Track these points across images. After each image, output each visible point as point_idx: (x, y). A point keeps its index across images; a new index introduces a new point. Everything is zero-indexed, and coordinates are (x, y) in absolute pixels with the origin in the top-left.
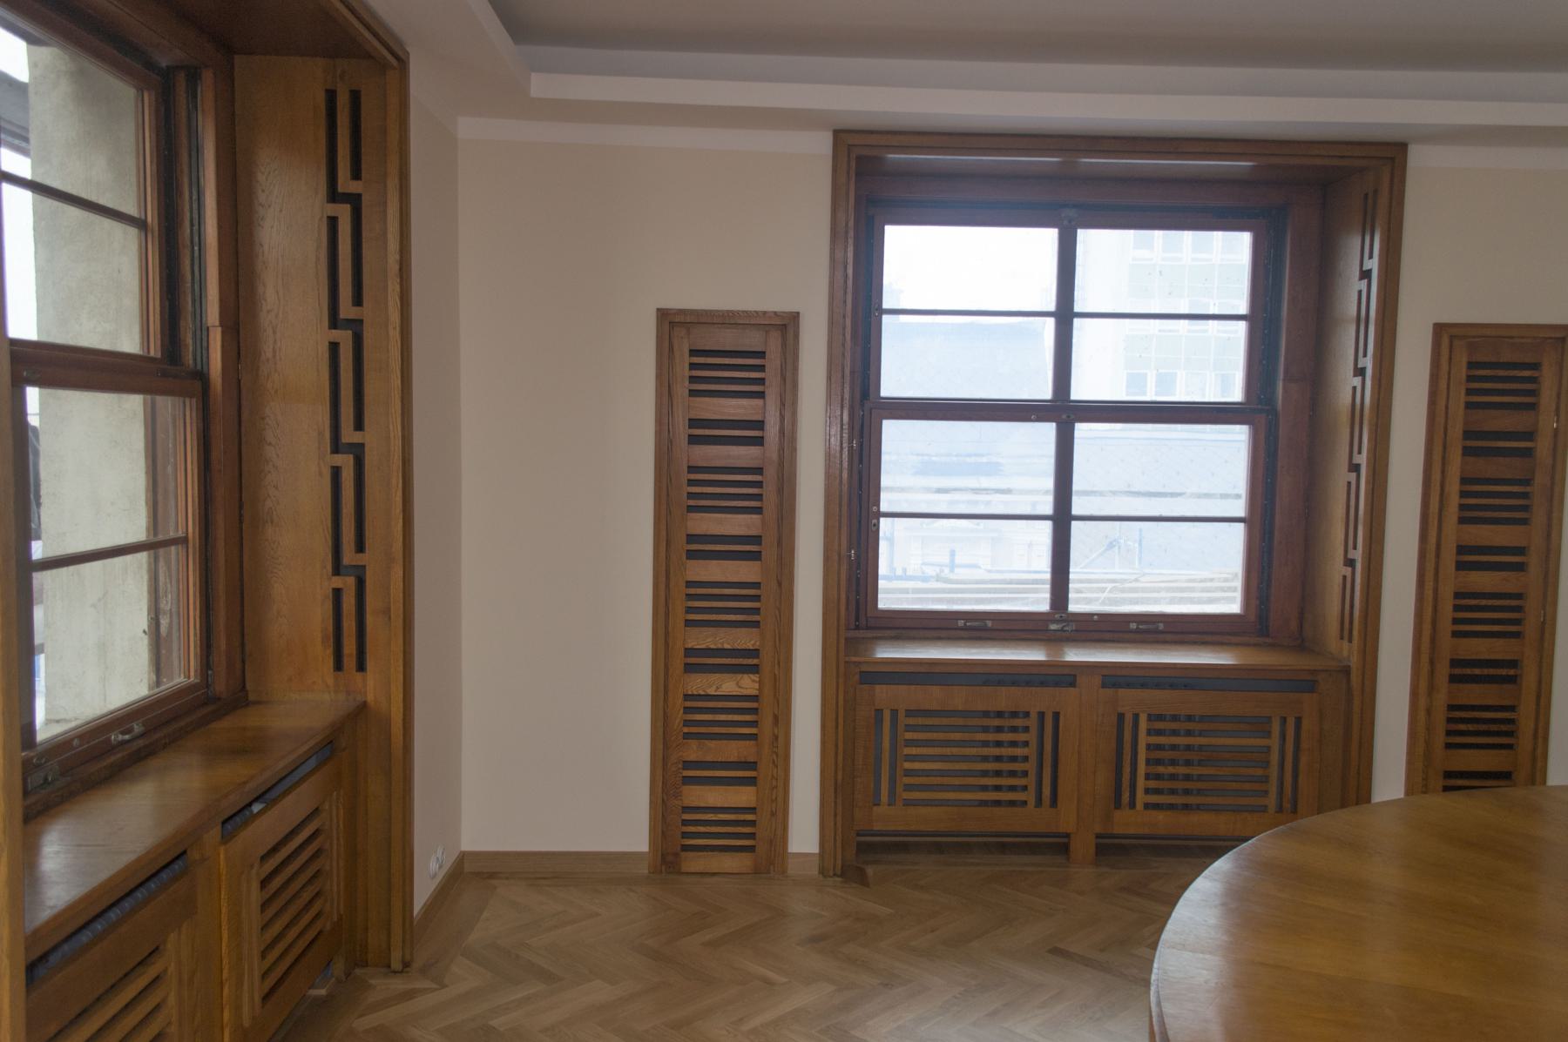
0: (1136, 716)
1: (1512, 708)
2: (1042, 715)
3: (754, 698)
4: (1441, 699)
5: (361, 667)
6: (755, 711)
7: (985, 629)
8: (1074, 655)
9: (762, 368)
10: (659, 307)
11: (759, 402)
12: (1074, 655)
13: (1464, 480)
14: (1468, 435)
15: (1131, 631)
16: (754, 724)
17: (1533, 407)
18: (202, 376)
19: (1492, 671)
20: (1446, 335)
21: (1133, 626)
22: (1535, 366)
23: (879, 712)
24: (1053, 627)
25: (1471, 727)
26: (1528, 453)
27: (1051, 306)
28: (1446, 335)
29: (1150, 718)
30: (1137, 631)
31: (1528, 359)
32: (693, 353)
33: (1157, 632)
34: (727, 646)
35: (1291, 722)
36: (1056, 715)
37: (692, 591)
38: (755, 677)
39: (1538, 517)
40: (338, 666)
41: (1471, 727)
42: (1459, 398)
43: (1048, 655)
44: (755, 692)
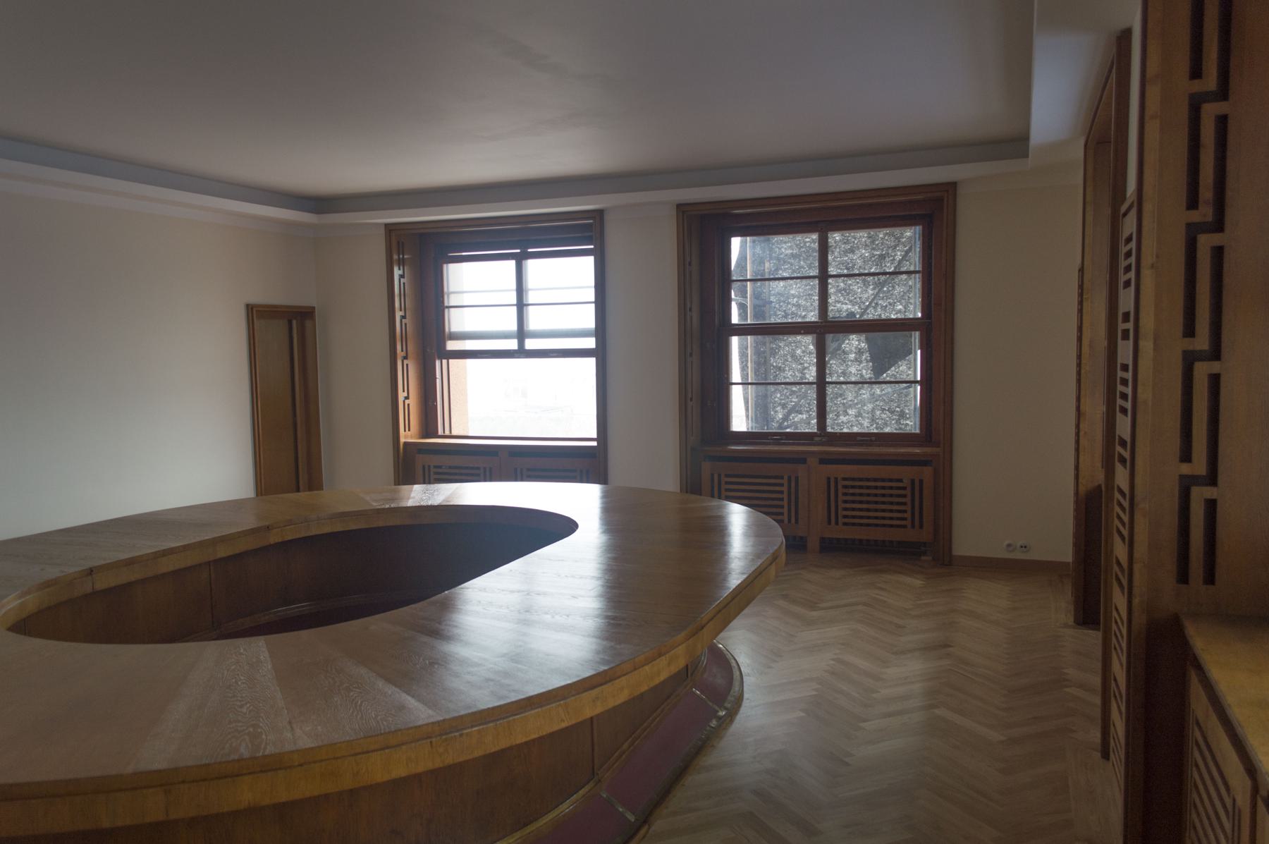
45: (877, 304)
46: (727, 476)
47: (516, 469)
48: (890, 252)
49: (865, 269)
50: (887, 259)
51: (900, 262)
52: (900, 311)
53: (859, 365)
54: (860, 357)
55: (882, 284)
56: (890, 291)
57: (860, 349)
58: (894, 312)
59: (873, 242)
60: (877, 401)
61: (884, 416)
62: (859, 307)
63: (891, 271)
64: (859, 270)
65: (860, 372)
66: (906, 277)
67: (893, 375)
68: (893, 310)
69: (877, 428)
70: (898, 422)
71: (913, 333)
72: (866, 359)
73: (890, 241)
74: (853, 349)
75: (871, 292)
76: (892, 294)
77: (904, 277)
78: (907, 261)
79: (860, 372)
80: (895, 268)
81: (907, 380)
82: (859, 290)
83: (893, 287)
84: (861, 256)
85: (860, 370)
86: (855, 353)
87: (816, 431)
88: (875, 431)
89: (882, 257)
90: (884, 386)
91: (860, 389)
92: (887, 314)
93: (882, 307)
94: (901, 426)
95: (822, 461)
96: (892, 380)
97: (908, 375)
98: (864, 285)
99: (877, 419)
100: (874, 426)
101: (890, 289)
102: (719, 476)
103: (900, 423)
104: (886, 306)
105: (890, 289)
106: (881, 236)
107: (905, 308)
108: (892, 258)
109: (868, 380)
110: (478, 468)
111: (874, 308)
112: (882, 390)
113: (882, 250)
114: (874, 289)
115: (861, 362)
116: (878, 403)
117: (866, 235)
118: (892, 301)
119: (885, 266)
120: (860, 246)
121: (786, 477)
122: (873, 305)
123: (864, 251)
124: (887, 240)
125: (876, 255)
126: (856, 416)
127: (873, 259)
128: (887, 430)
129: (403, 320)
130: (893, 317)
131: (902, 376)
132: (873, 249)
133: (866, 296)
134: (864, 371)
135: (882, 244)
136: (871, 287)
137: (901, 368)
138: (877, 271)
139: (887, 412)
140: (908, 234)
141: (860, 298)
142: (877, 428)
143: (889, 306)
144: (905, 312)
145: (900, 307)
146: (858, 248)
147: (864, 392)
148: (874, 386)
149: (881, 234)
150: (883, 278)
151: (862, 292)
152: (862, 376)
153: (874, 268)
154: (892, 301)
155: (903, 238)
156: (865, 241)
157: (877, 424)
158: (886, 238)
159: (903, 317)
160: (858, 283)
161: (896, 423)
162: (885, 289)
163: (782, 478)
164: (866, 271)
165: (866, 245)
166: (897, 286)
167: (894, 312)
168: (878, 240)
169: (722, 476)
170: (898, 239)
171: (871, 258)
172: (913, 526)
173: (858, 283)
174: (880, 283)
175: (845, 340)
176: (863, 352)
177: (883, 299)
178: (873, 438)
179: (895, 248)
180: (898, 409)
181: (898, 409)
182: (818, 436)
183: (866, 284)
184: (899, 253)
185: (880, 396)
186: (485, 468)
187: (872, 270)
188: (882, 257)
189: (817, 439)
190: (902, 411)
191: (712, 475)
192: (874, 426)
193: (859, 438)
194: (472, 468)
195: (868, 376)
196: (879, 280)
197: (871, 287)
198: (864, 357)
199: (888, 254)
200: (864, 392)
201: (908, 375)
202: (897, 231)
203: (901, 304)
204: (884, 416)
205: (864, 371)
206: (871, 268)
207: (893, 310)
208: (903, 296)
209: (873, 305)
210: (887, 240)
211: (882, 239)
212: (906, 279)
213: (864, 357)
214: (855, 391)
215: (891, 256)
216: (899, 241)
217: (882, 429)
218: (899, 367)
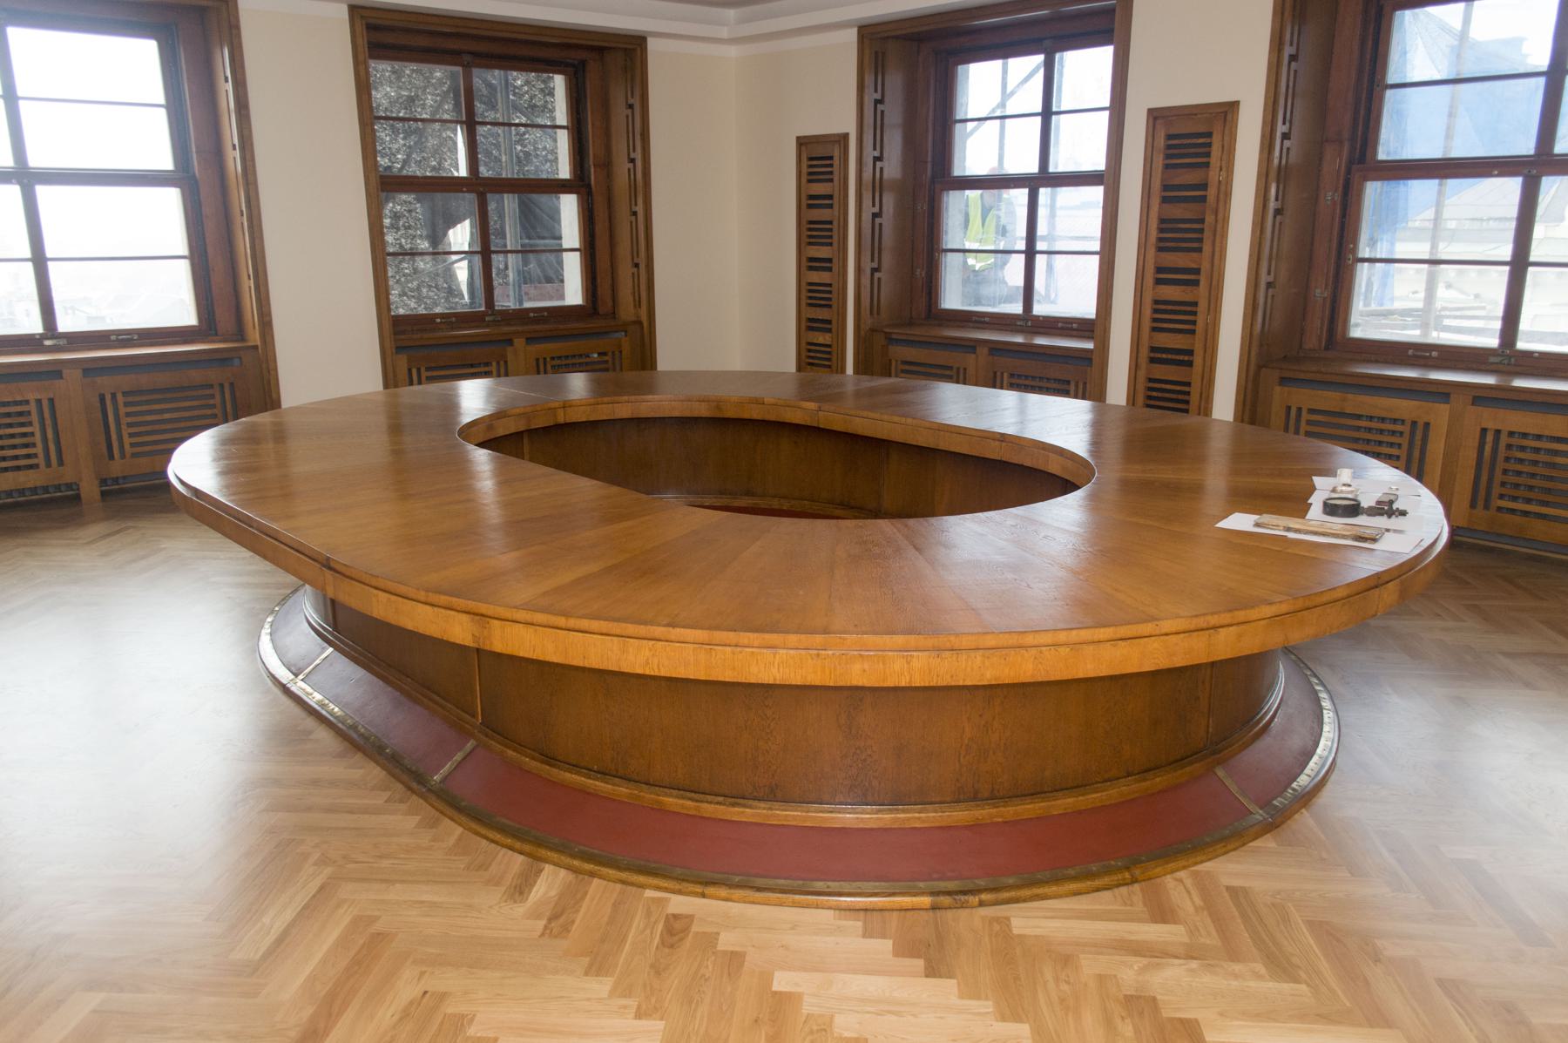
0: (1002, 374)
1: (1188, 384)
2: (958, 369)
3: (829, 346)
4: (1142, 374)
5: (640, 307)
6: (829, 353)
7: (984, 322)
8: (1041, 341)
9: (831, 166)
10: (799, 135)
11: (830, 184)
12: (1041, 341)
13: (1162, 221)
14: (1165, 187)
15: (1058, 329)
16: (829, 360)
17: (1207, 165)
18: (589, 185)
19: (1174, 357)
20: (1155, 116)
21: (1060, 325)
22: (1209, 135)
23: (890, 360)
24: (1019, 323)
25: (1160, 395)
26: (1203, 199)
27: (1039, 109)
28: (1155, 116)
29: (1012, 375)
30: (1062, 328)
31: (1202, 129)
32: (811, 159)
33: (1072, 329)
34: (820, 318)
35: (1081, 386)
36: (965, 369)
37: (828, 289)
38: (830, 335)
39: (1207, 248)
40: (635, 306)
41: (1160, 395)
42: (1159, 161)
43: (1025, 339)
44: (829, 343)
46: (428, 369)
47: (102, 398)
48: (420, 94)
49: (392, 112)
52: (434, 168)
53: (396, 233)
54: (397, 223)
57: (396, 213)
59: (399, 78)
61: (431, 294)
62: (390, 160)
64: (385, 112)
65: (398, 242)
66: (438, 127)
69: (425, 308)
70: (447, 299)
71: (506, 195)
72: (404, 226)
73: (419, 82)
74: (387, 212)
75: (402, 142)
77: (437, 126)
79: (398, 242)
80: (433, 113)
82: (388, 139)
84: (386, 95)
85: (398, 239)
86: (390, 217)
87: (483, 309)
88: (424, 312)
91: (400, 262)
94: (451, 305)
95: (530, 340)
98: (393, 132)
99: (424, 298)
100: (423, 306)
102: (419, 370)
103: (450, 301)
104: (420, 161)
106: (408, 72)
107: (440, 165)
108: (422, 102)
110: (27, 402)
112: (425, 264)
114: (404, 139)
115: (398, 229)
117: (389, 69)
119: (416, 111)
120: (384, 82)
121: (494, 364)
123: (388, 89)
126: (400, 295)
127: (401, 100)
128: (438, 310)
129: (878, 163)
130: (428, 174)
132: (400, 88)
133: (396, 146)
134: (403, 241)
135: (410, 83)
136: (401, 136)
138: (407, 116)
139: (435, 290)
140: (438, 74)
141: (390, 148)
142: (425, 308)
144: (439, 169)
145: (434, 163)
146: (382, 85)
147: (406, 266)
149: (409, 68)
151: (391, 142)
152: (401, 246)
153: (403, 111)
155: (433, 78)
156: (389, 77)
157: (426, 303)
158: (414, 75)
159: (437, 175)
160: (385, 129)
161: (446, 301)
163: (487, 364)
164: (394, 115)
165: (391, 82)
166: (430, 137)
167: (429, 169)
168: (404, 77)
169: (423, 369)
170: (427, 79)
171: (398, 98)
172: (49, 465)
173: (385, 129)
175: (387, 201)
176: (399, 217)
178: (454, 319)
180: (445, 285)
181: (445, 285)
182: (490, 315)
183: (395, 132)
186: (39, 402)
187: (401, 115)
188: (411, 100)
189: (487, 319)
190: (450, 287)
191: (410, 370)
192: (423, 306)
193: (532, 315)
194: (16, 403)
195: (409, 246)
196: (410, 127)
197: (401, 136)
198: (401, 223)
200: (406, 266)
202: (425, 67)
203: (435, 160)
204: (431, 294)
205: (403, 241)
206: (399, 112)
208: (437, 150)
210: (415, 78)
213: (401, 223)
214: (396, 266)
216: (429, 82)
217: (431, 309)
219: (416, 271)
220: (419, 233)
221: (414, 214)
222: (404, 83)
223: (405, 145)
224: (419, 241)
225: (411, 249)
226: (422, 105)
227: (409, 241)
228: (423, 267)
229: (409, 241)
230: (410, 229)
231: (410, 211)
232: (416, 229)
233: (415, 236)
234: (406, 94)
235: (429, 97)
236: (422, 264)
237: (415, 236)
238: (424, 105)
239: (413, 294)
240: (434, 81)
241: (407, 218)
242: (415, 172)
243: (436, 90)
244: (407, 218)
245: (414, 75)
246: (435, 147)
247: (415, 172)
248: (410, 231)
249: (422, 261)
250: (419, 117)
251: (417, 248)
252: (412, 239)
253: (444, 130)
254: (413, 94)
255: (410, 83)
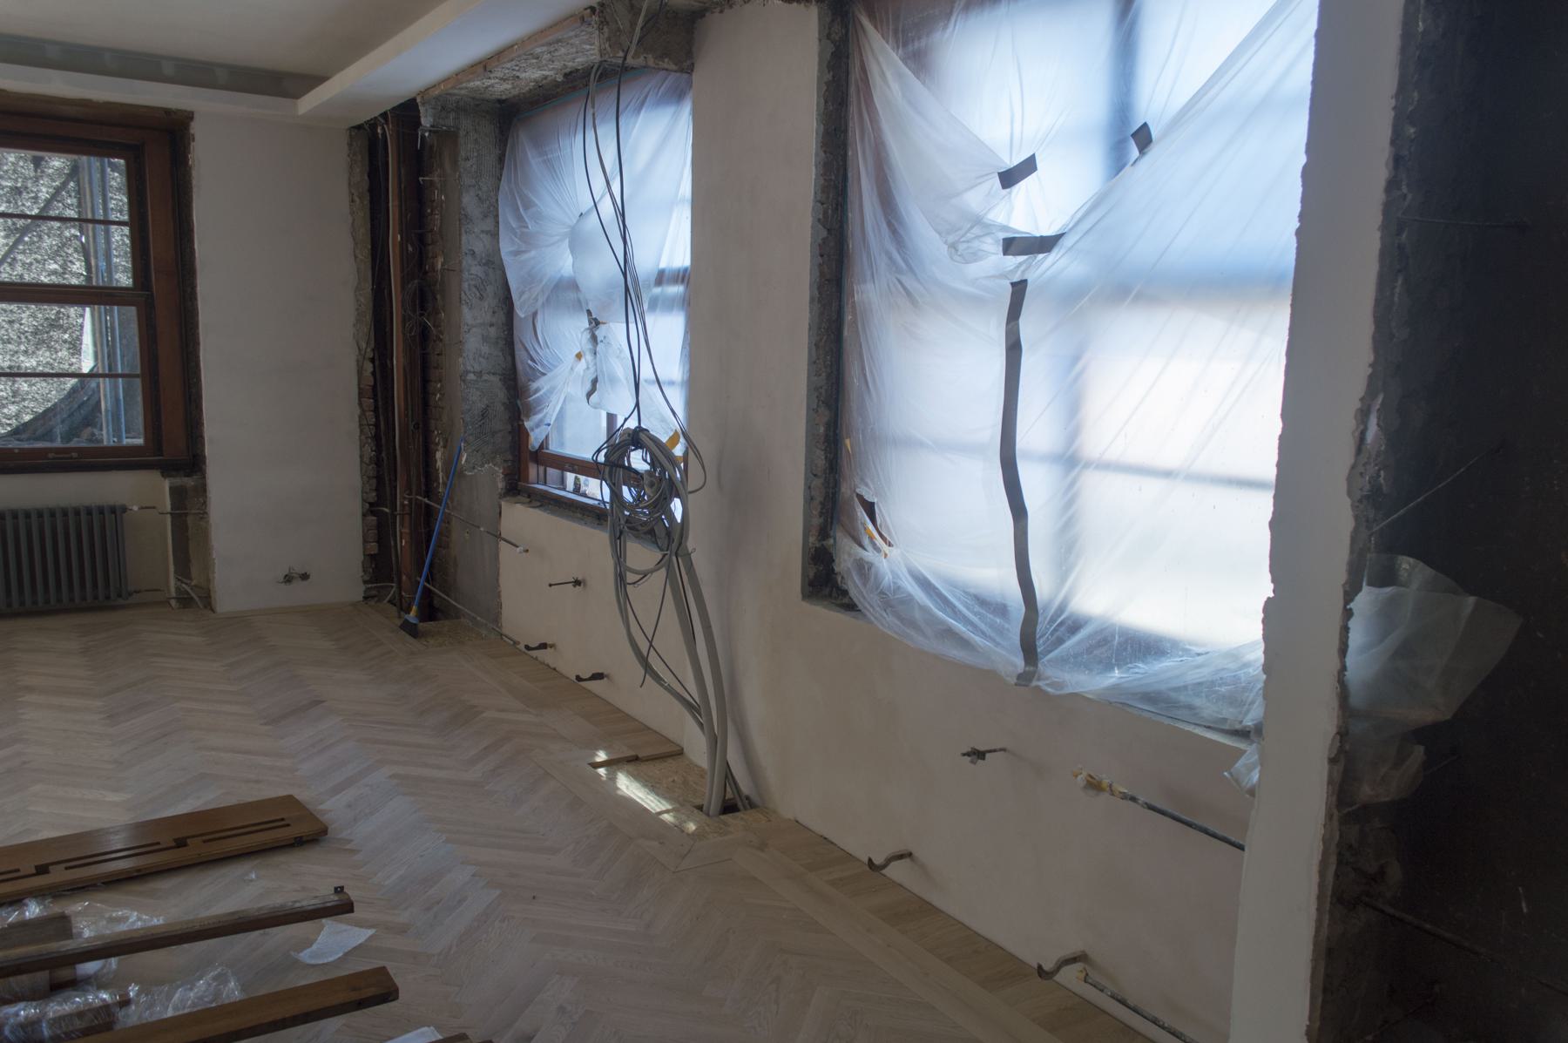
45: (14, 259)
48: (29, 185)
50: (24, 195)
51: (48, 202)
55: (24, 231)
56: (34, 243)
58: (44, 273)
60: (24, 400)
63: (33, 213)
67: (48, 363)
68: (44, 269)
73: (28, 169)
76: (39, 248)
78: (59, 201)
80: (42, 210)
81: (70, 371)
83: (40, 237)
89: (17, 191)
90: (34, 380)
92: (32, 276)
93: (24, 264)
96: (47, 370)
97: (71, 365)
101: (35, 239)
104: (31, 264)
105: (35, 239)
108: (33, 195)
109: (8, 371)
111: (10, 264)
112: (30, 386)
113: (16, 180)
116: (26, 404)
118: (39, 257)
119: (23, 205)
122: (9, 260)
124: (22, 167)
125: (7, 186)
131: (61, 366)
135: (15, 171)
137: (60, 354)
138: (10, 211)
143: (35, 265)
148: (18, 379)
150: (21, 223)
154: (39, 257)
162: (26, 239)
168: (7, 164)
174: (16, 229)
177: (24, 252)
179: (37, 179)
184: (44, 190)
185: (27, 393)
188: (17, 191)
196: (14, 224)
199: (27, 188)
201: (71, 365)
207: (44, 269)
209: (9, 260)
210: (22, 167)
211: (13, 163)
212: (59, 227)
215: (32, 191)
218: (56, 352)
219: (15, 393)
220: (23, 348)
221: (16, 326)
222: (7, 171)
223: (7, 244)
224: (22, 358)
225: (10, 367)
226: (33, 198)
227: (8, 357)
228: (26, 389)
229: (8, 357)
230: (10, 343)
231: (11, 322)
232: (20, 344)
233: (16, 352)
234: (9, 184)
235: (44, 190)
236: (25, 385)
237: (16, 352)
238: (36, 198)
239: (8, 422)
240: (50, 171)
241: (7, 330)
242: (21, 276)
243: (55, 182)
244: (7, 330)
245: (21, 164)
246: (56, 248)
247: (21, 276)
248: (10, 346)
249: (26, 382)
250: (28, 213)
251: (19, 367)
252: (13, 355)
253: (67, 228)
254: (19, 185)
255: (15, 171)
